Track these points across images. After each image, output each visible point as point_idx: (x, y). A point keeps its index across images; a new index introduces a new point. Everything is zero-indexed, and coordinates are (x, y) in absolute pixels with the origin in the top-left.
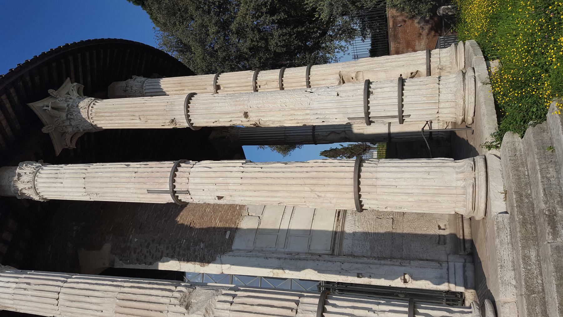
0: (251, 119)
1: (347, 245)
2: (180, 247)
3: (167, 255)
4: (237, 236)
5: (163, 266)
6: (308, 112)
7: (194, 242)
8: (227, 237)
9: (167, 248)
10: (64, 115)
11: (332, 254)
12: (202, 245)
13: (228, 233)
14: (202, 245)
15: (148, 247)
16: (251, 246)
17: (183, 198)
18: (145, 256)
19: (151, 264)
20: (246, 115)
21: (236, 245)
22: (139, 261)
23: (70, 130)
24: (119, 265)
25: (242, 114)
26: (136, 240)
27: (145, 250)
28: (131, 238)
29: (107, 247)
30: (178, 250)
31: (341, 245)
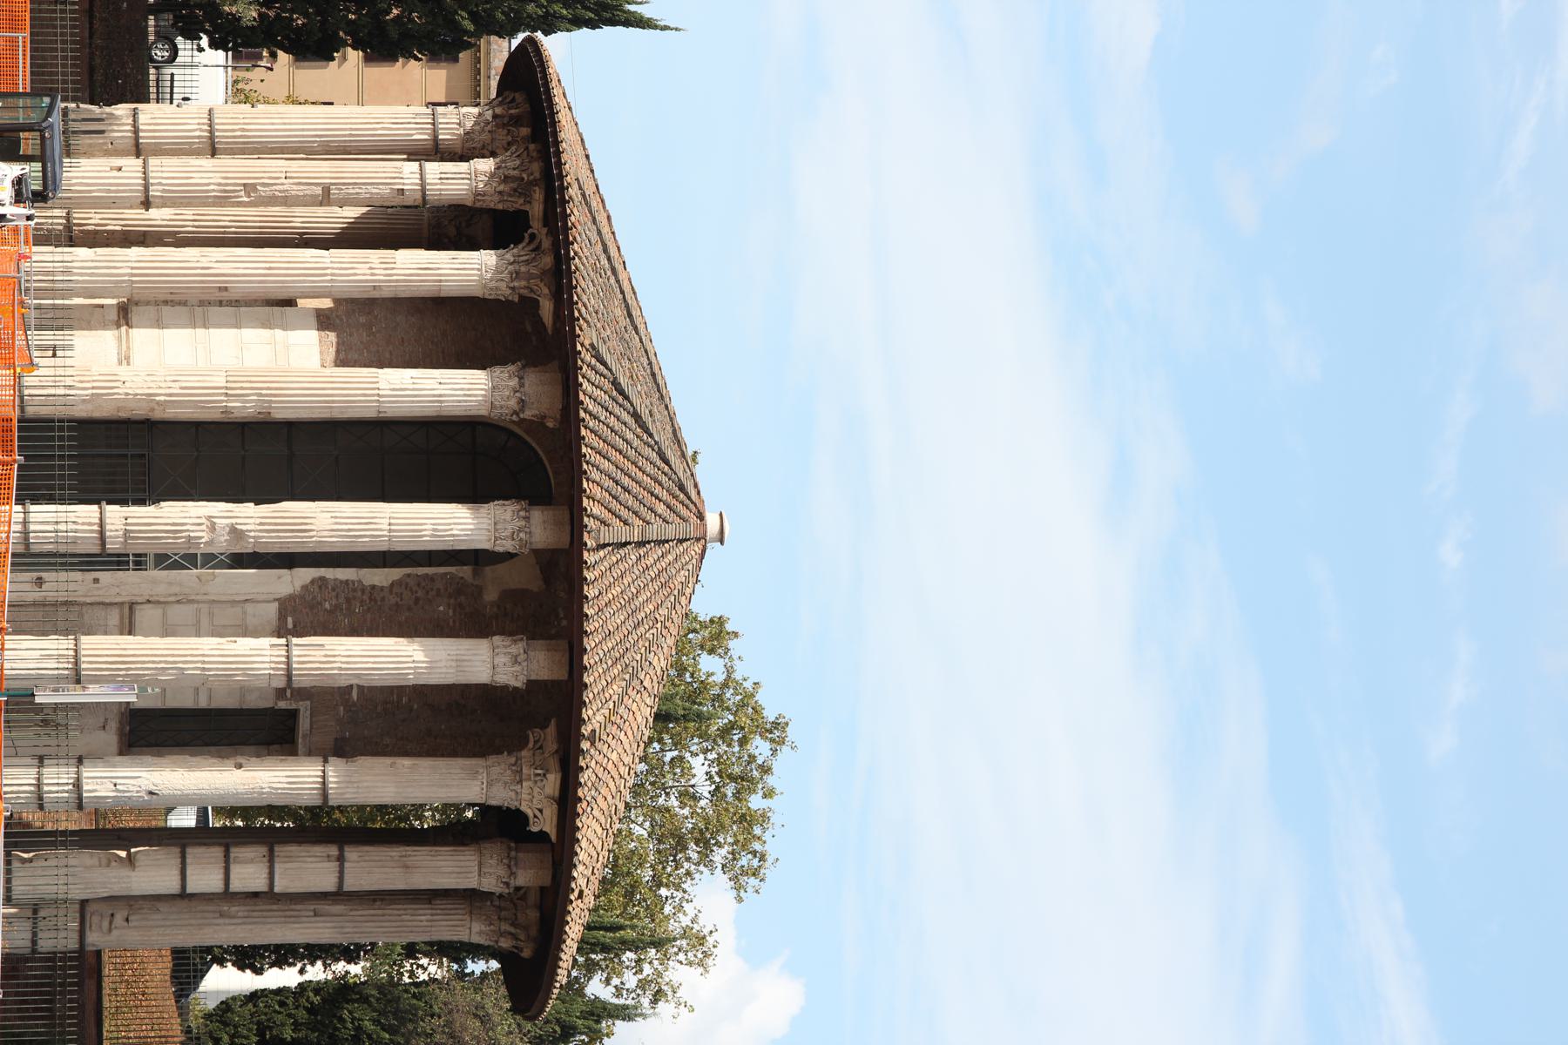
1: (114, 617)
3: (382, 589)
4: (275, 622)
5: (395, 574)
8: (290, 620)
9: (383, 599)
10: (525, 771)
11: (132, 605)
12: (327, 606)
13: (290, 626)
14: (327, 606)
15: (417, 599)
16: (249, 608)
17: (283, 641)
22: (431, 578)
23: (524, 753)
24: (465, 572)
27: (419, 594)
29: (491, 595)
31: (122, 618)
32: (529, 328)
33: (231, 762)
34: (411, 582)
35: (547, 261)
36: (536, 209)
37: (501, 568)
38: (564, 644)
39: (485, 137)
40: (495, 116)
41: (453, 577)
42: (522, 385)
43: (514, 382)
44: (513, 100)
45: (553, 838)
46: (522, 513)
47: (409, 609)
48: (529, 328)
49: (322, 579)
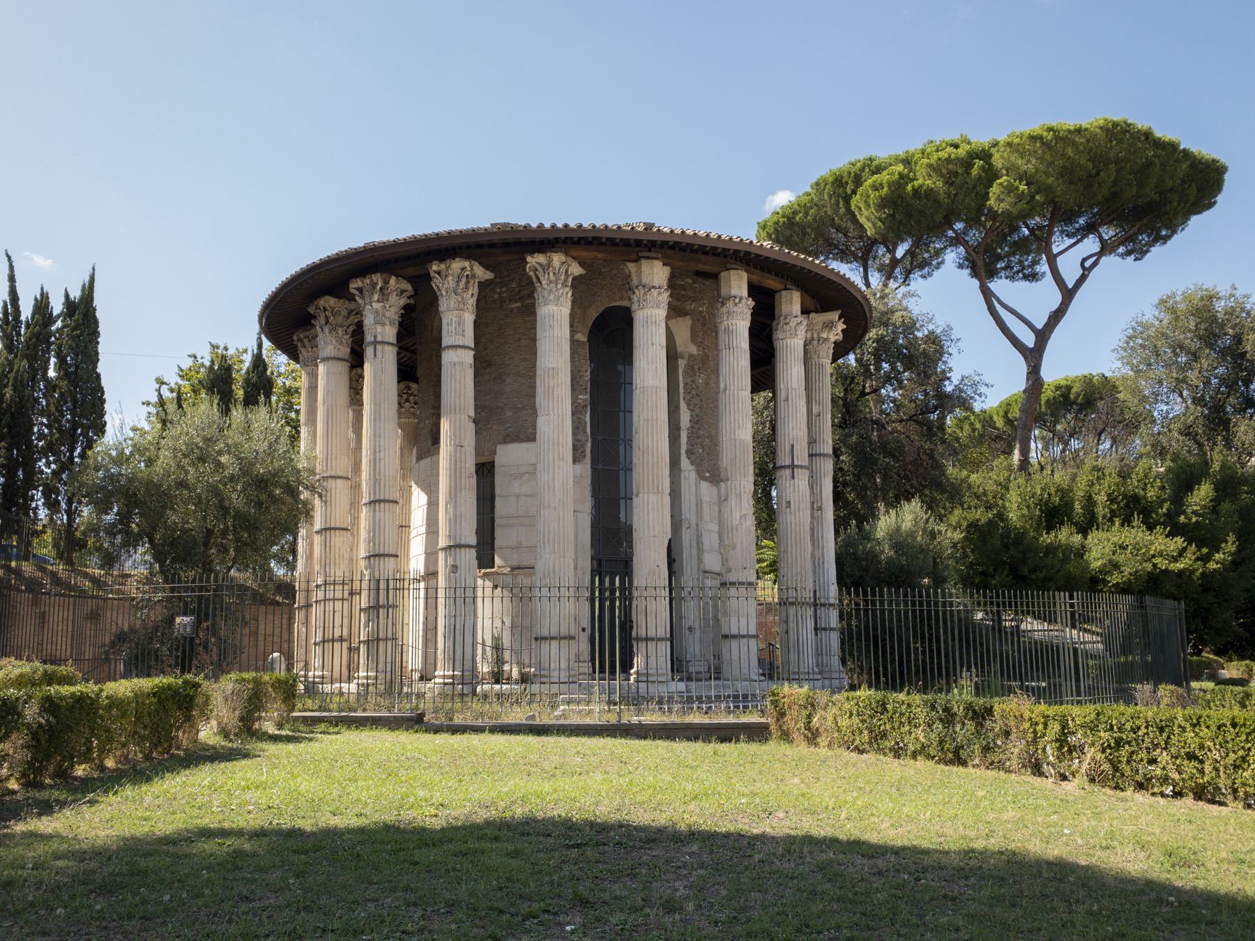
10: (824, 335)
21: (704, 485)
22: (686, 384)
24: (682, 363)
29: (693, 350)
32: (518, 305)
34: (688, 397)
35: (557, 259)
37: (679, 341)
38: (784, 293)
39: (393, 310)
41: (684, 372)
43: (655, 292)
48: (518, 305)
49: (687, 452)
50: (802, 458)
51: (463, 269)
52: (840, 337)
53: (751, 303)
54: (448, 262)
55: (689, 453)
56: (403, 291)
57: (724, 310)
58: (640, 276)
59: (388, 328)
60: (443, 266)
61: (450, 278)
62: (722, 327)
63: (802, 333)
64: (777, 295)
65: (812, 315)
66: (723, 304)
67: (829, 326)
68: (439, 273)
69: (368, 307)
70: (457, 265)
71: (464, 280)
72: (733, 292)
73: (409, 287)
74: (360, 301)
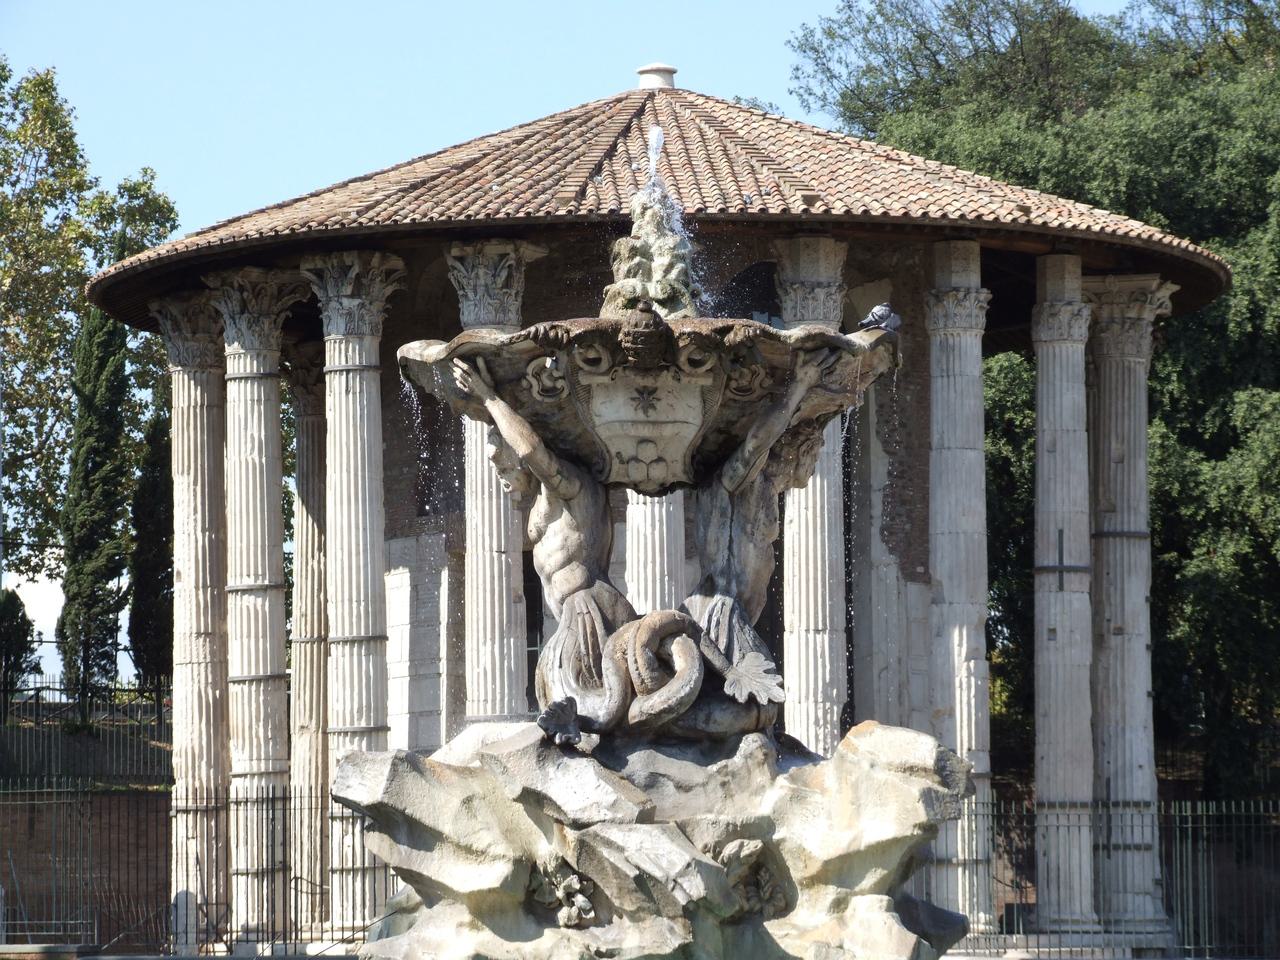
0: (1113, 637)
2: (904, 487)
6: (1120, 725)
7: (911, 511)
10: (1132, 314)
14: (908, 527)
18: (887, 422)
19: (878, 433)
20: (1120, 631)
22: (881, 406)
25: (1119, 624)
26: (908, 397)
28: (912, 387)
30: (900, 483)
33: (1114, 641)
36: (531, 252)
38: (1052, 259)
39: (377, 306)
40: (352, 296)
42: (819, 285)
43: (820, 293)
44: (319, 274)
45: (1176, 288)
46: (961, 295)
47: (909, 434)
49: (882, 530)
50: (1078, 550)
51: (503, 256)
52: (1167, 310)
53: (985, 295)
54: (479, 246)
55: (888, 531)
56: (389, 273)
57: (939, 311)
58: (796, 264)
59: (368, 340)
60: (469, 250)
61: (481, 272)
62: (936, 340)
63: (1081, 329)
64: (1039, 260)
65: (1110, 279)
66: (939, 299)
67: (1141, 297)
68: (461, 259)
69: (334, 304)
70: (493, 249)
71: (504, 274)
72: (956, 280)
73: (397, 263)
74: (319, 294)
